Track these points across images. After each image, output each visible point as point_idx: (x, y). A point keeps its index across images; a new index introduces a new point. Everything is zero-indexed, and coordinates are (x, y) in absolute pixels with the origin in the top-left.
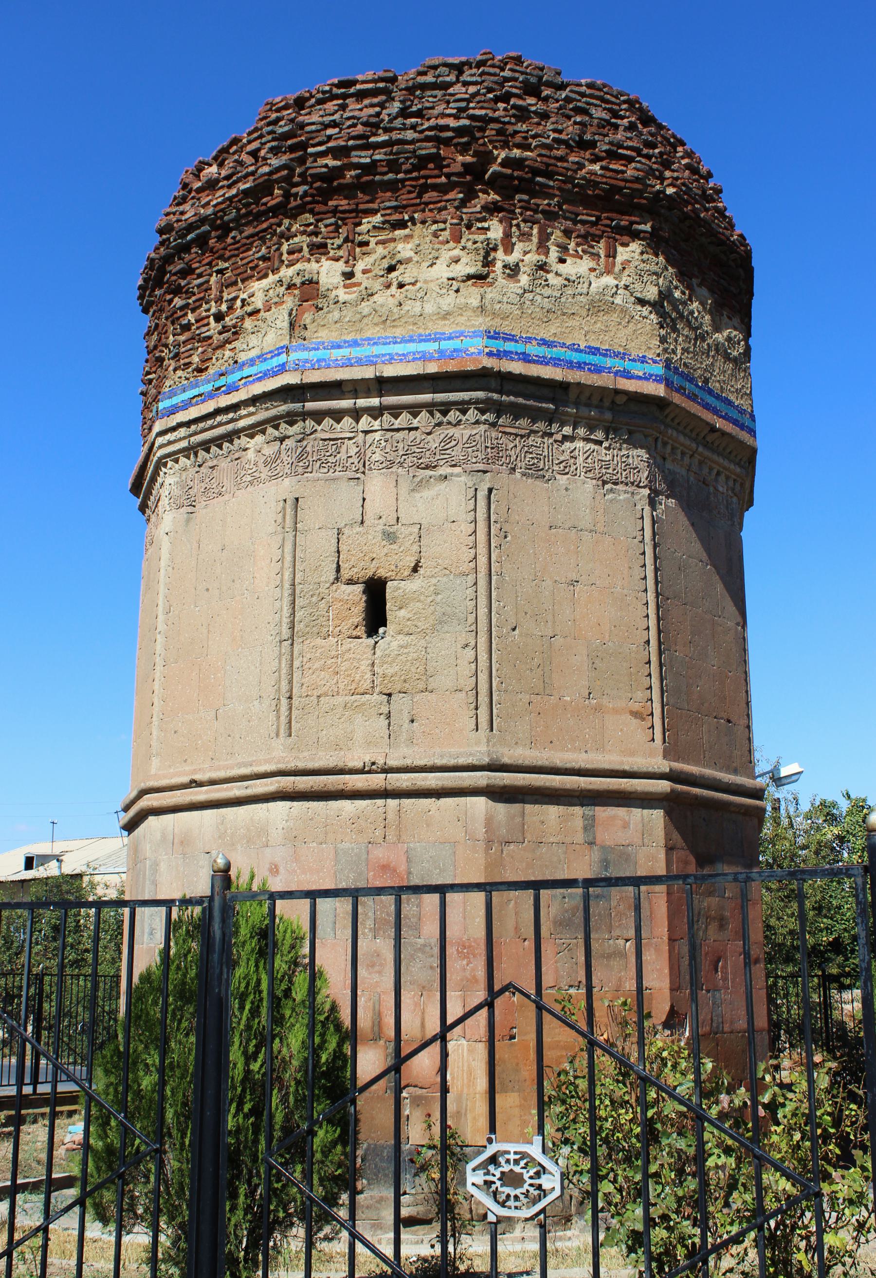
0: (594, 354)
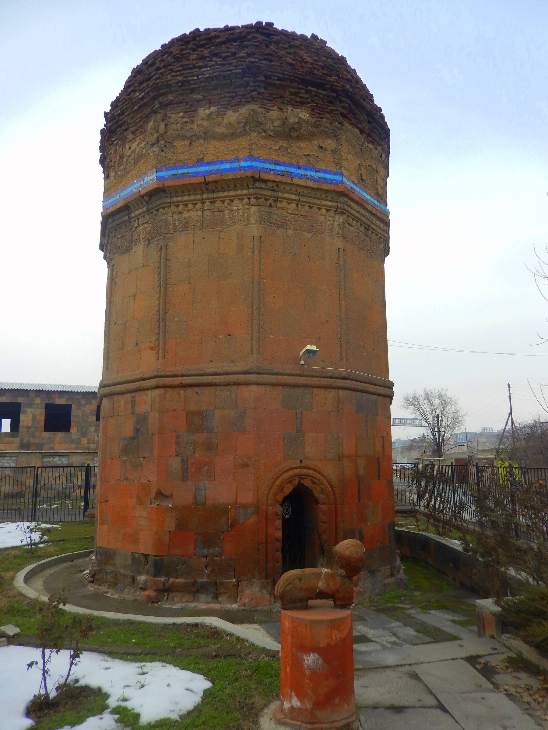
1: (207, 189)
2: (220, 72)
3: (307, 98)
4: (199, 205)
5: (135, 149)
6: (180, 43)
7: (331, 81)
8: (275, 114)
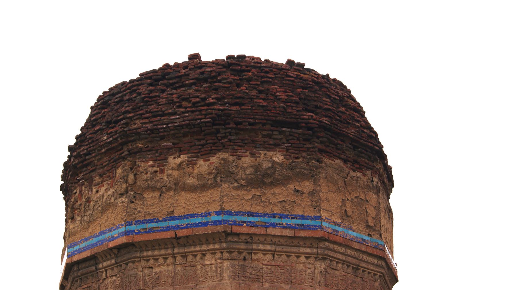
0: (101, 235)
1: (178, 243)
2: (190, 120)
3: (281, 139)
4: (170, 260)
5: (103, 196)
6: (149, 81)
7: (306, 119)
8: (247, 161)
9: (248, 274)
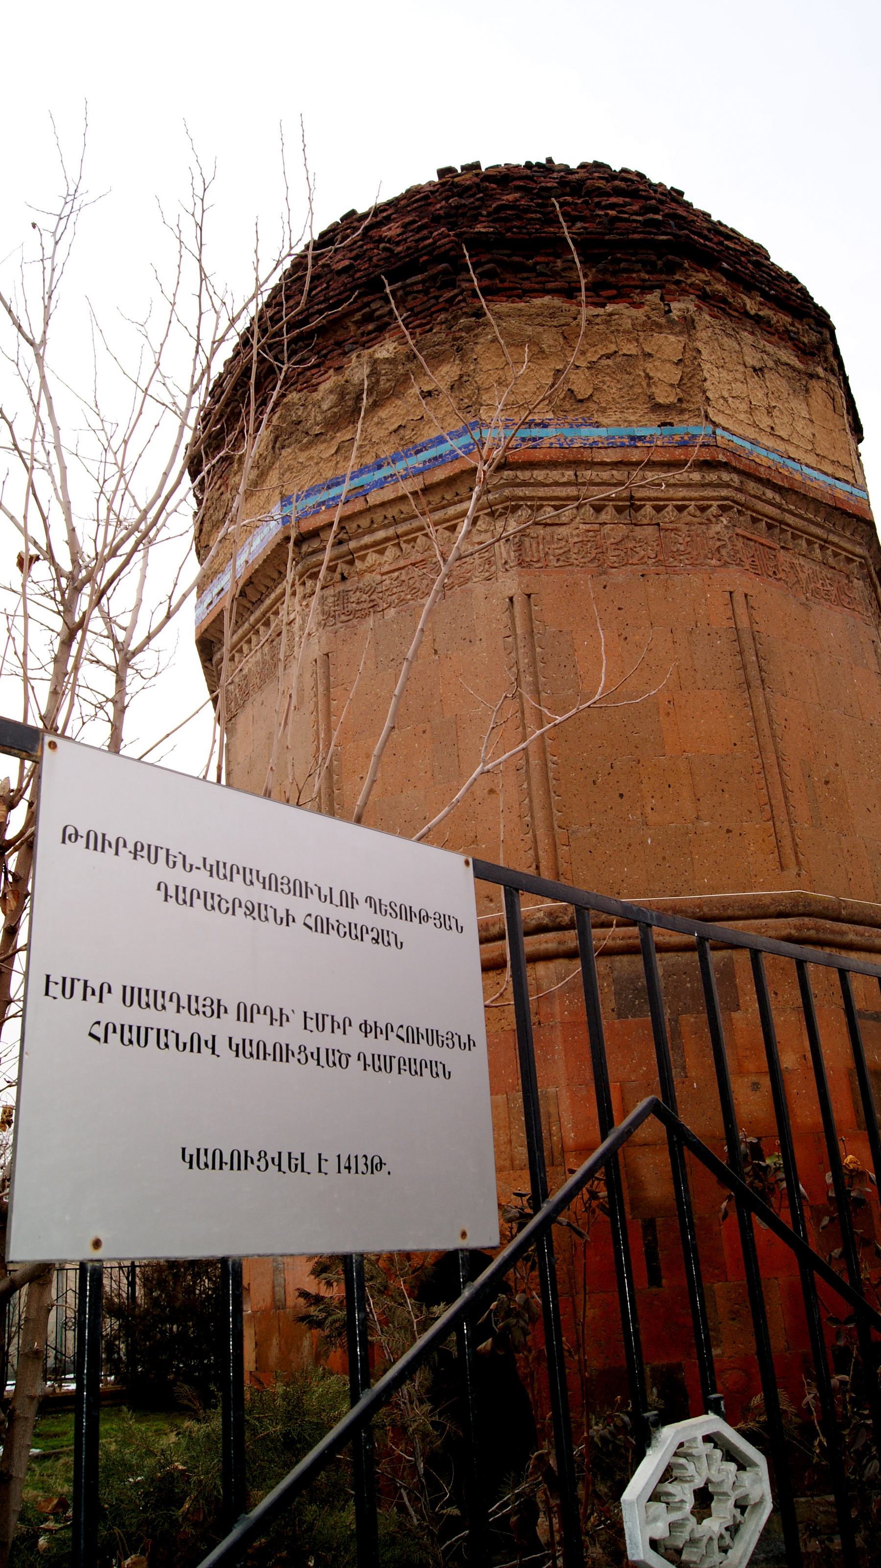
9: (354, 605)
